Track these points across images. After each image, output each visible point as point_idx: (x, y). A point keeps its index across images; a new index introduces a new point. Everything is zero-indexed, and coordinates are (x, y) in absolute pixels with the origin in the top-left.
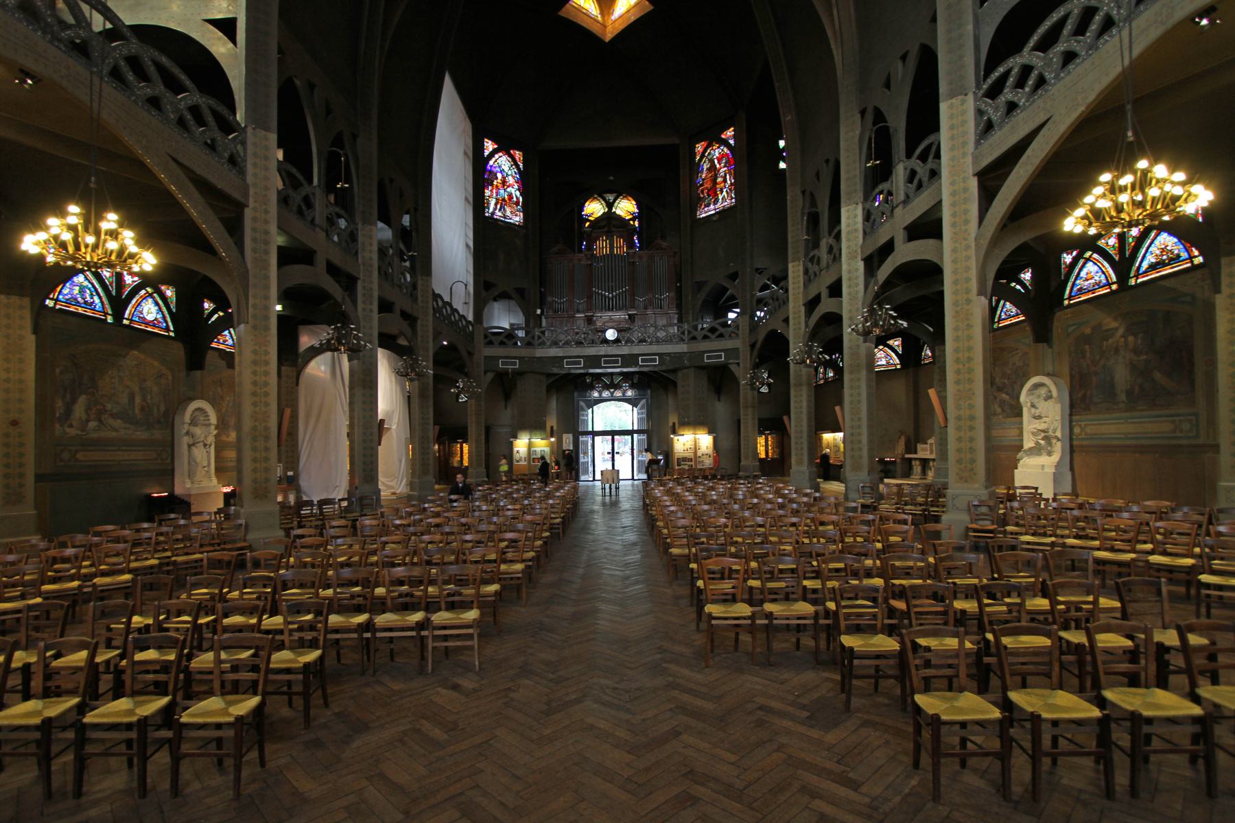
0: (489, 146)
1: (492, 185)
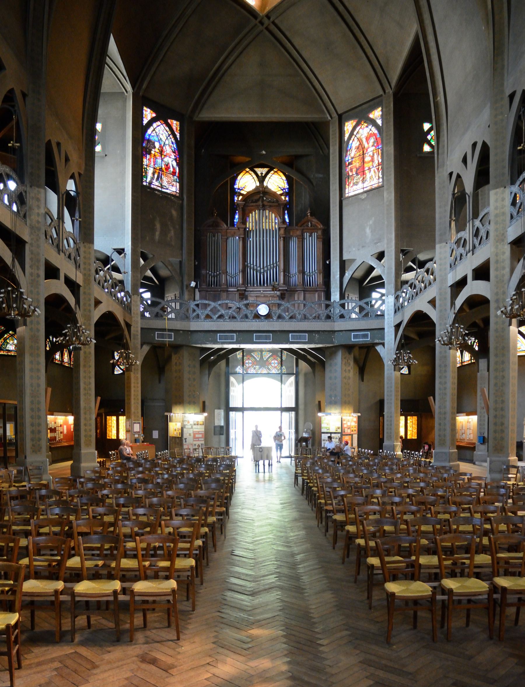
0: (148, 114)
1: (150, 154)
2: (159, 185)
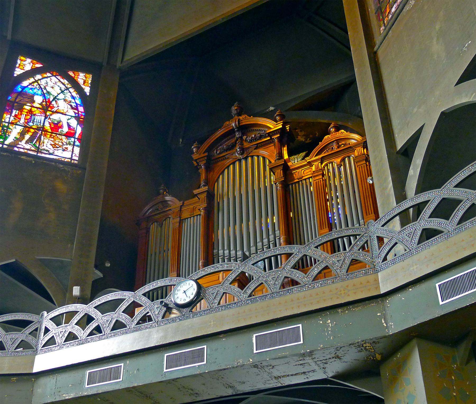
2: (33, 149)
